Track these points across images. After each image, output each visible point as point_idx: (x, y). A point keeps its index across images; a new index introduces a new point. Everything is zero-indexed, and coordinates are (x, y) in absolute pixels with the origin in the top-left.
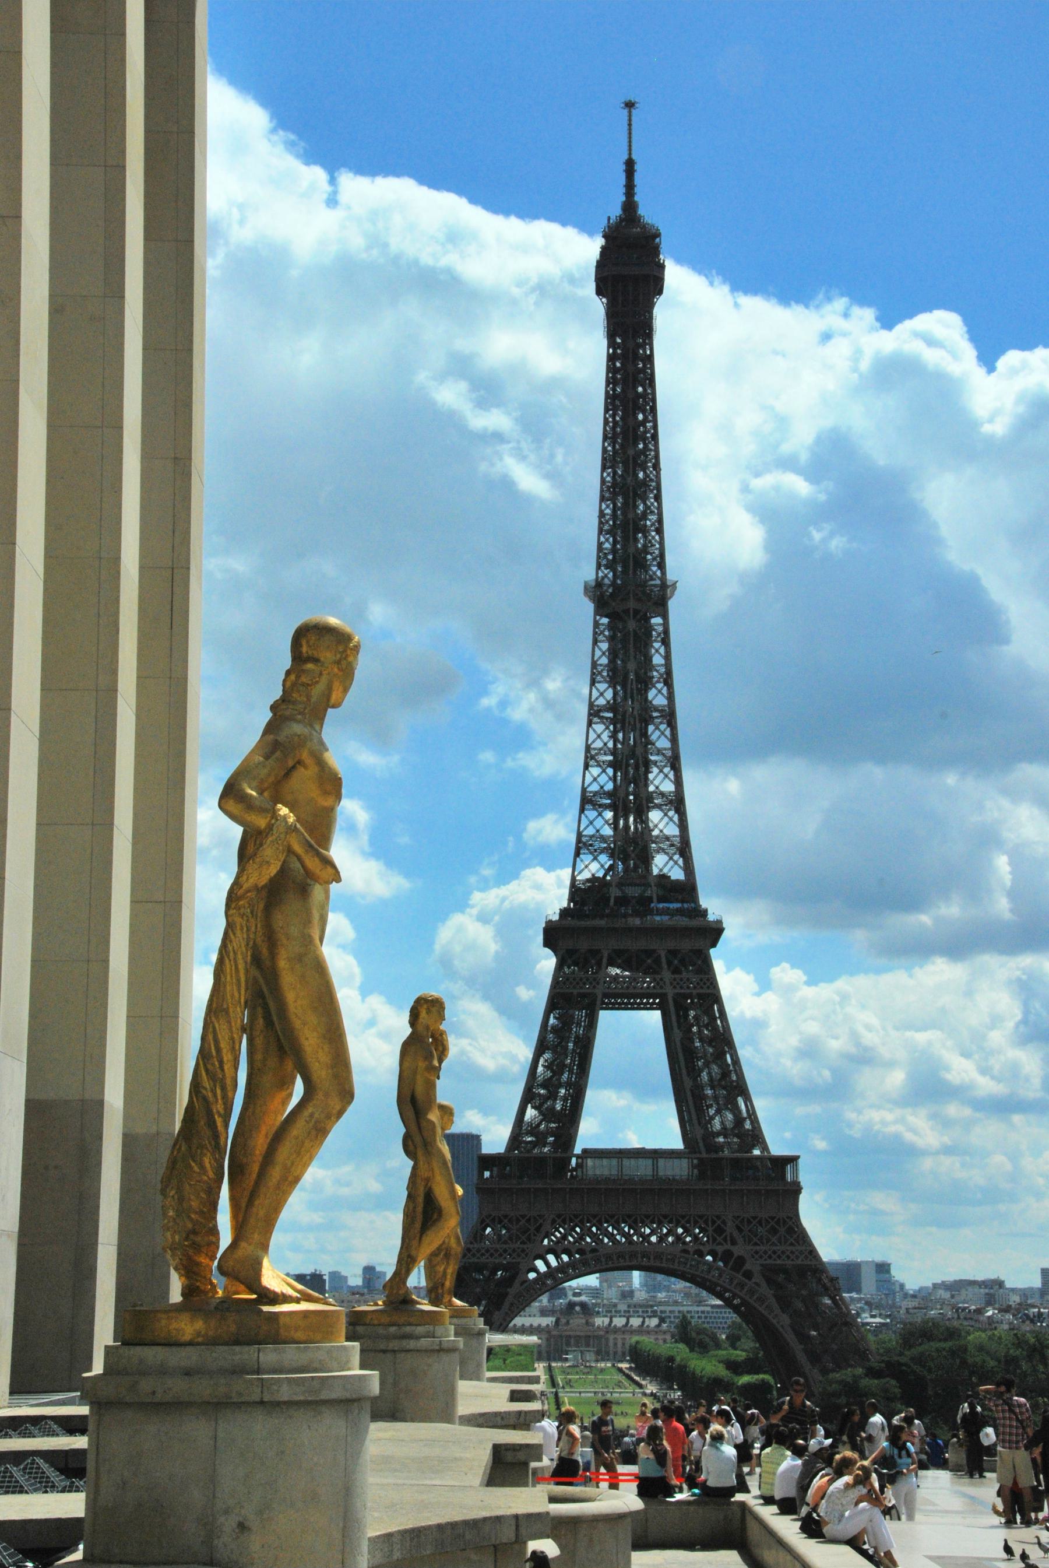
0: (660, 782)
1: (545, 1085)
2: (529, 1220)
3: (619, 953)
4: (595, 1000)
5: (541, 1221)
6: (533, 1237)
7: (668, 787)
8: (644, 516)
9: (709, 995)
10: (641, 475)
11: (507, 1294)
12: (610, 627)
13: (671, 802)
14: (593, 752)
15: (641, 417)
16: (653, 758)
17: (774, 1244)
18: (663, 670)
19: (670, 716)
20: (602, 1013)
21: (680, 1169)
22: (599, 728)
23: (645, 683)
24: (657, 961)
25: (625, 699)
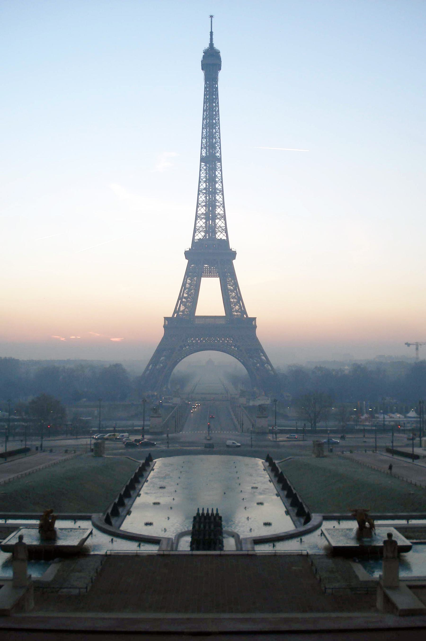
0: (219, 211)
1: (185, 298)
7: (222, 212)
8: (215, 134)
10: (214, 121)
12: (205, 166)
13: (223, 217)
14: (199, 202)
15: (214, 105)
16: (217, 204)
18: (220, 178)
19: (222, 191)
20: (202, 278)
21: (223, 322)
22: (201, 195)
25: (209, 187)
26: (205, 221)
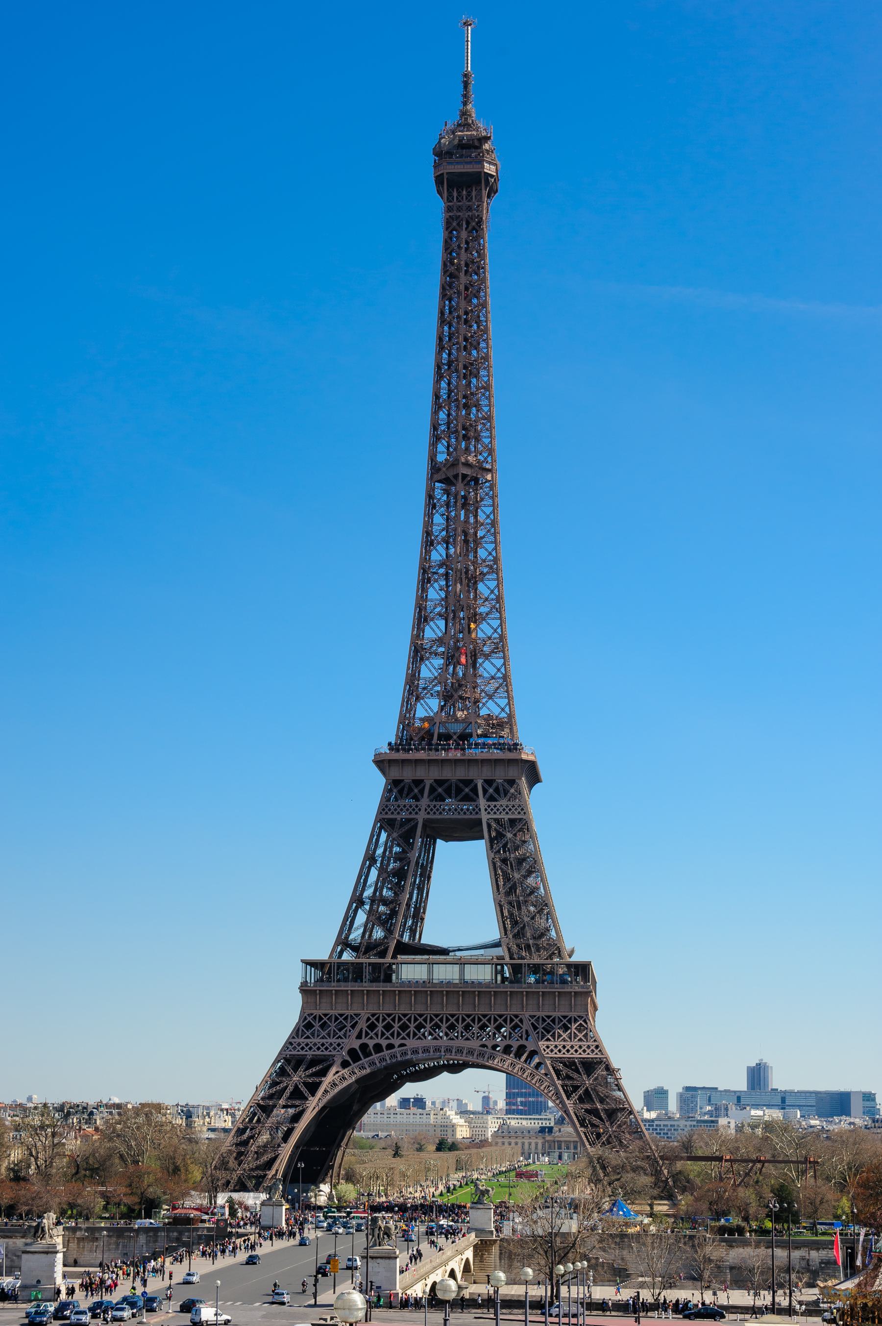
2: (346, 1019)
3: (440, 782)
4: (417, 823)
5: (357, 1019)
6: (348, 1033)
9: (520, 820)
11: (321, 1082)
12: (447, 492)
17: (564, 1040)
23: (471, 542)
24: (475, 790)
26: (442, 661)
